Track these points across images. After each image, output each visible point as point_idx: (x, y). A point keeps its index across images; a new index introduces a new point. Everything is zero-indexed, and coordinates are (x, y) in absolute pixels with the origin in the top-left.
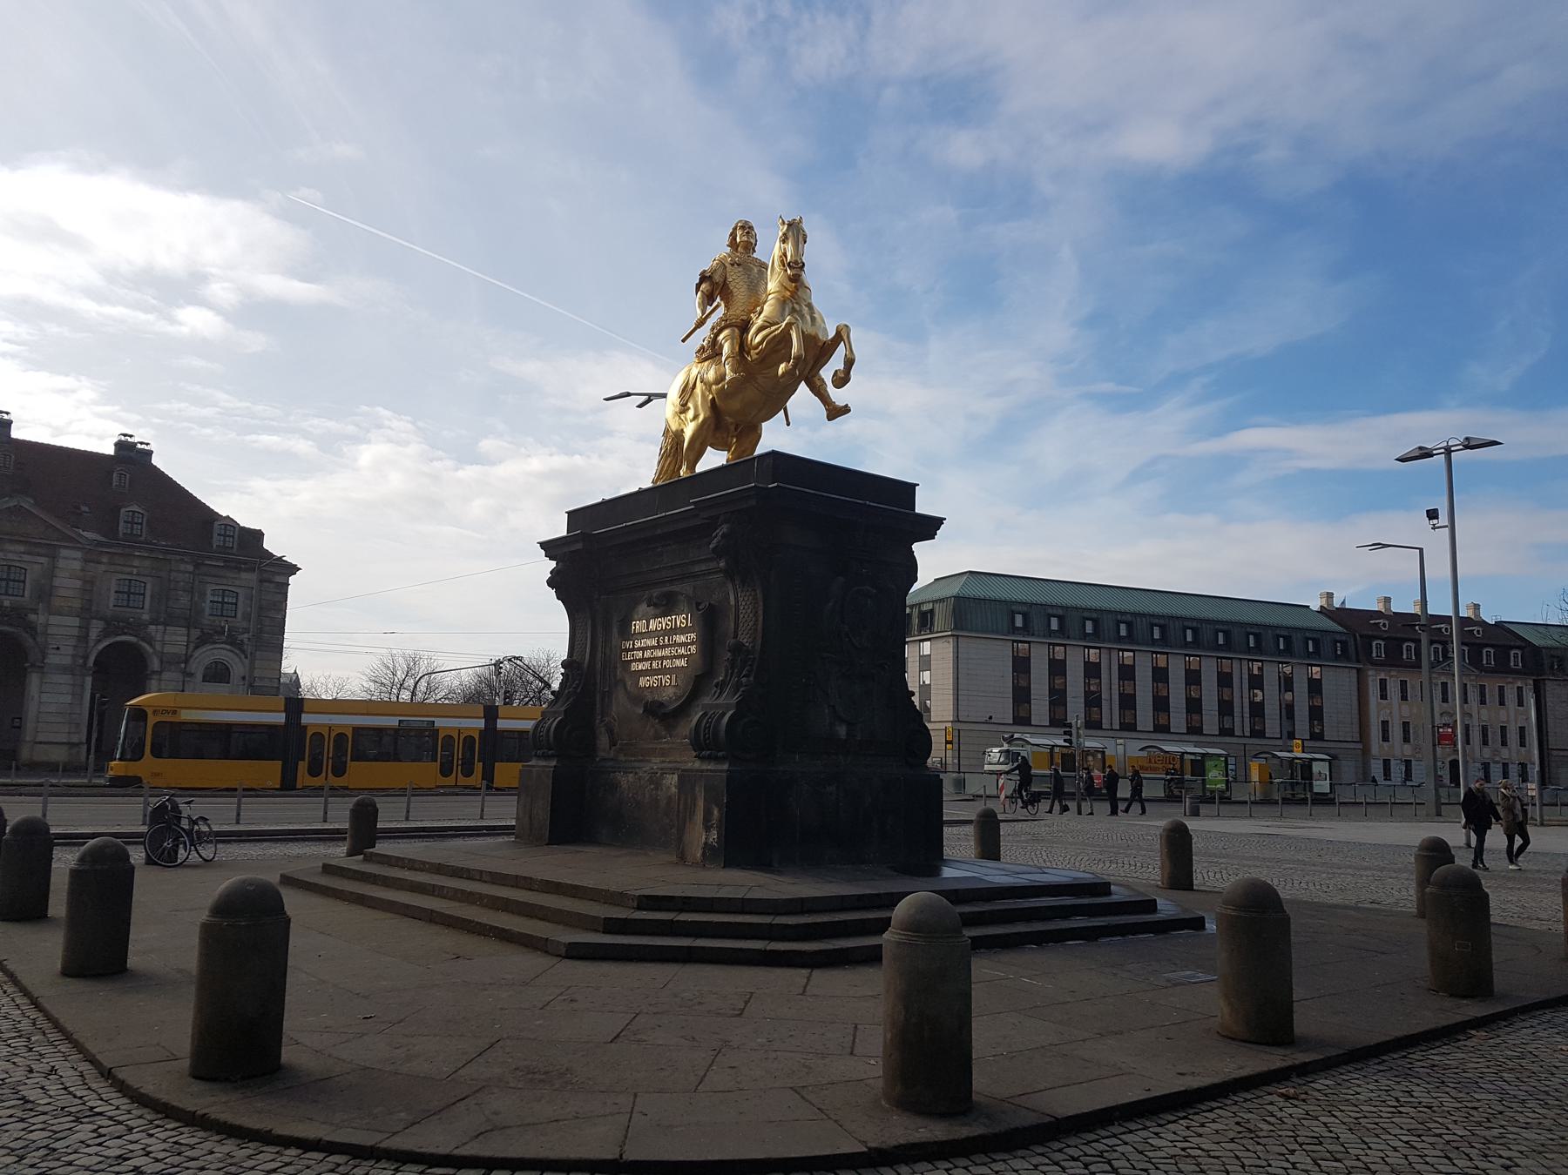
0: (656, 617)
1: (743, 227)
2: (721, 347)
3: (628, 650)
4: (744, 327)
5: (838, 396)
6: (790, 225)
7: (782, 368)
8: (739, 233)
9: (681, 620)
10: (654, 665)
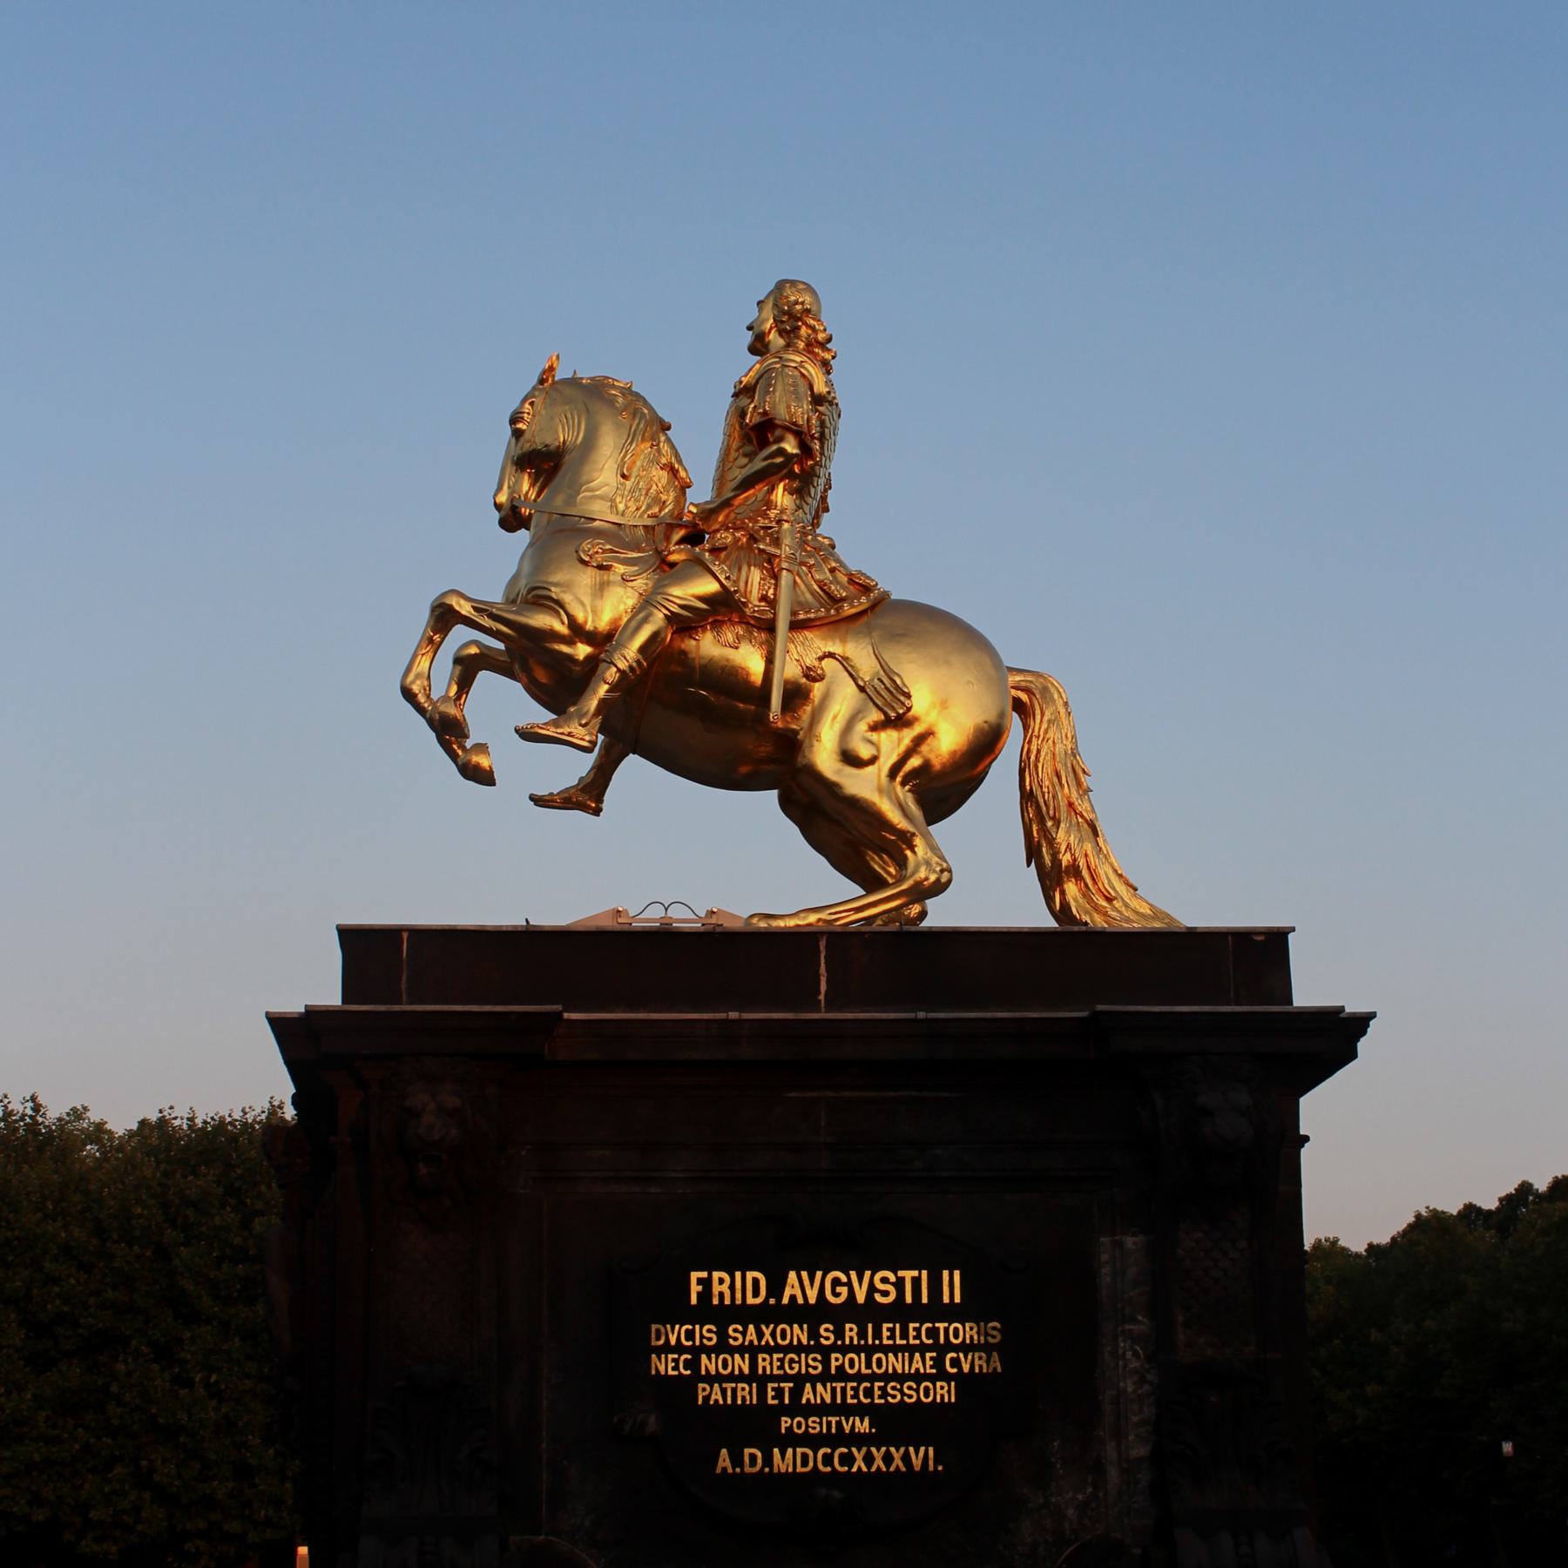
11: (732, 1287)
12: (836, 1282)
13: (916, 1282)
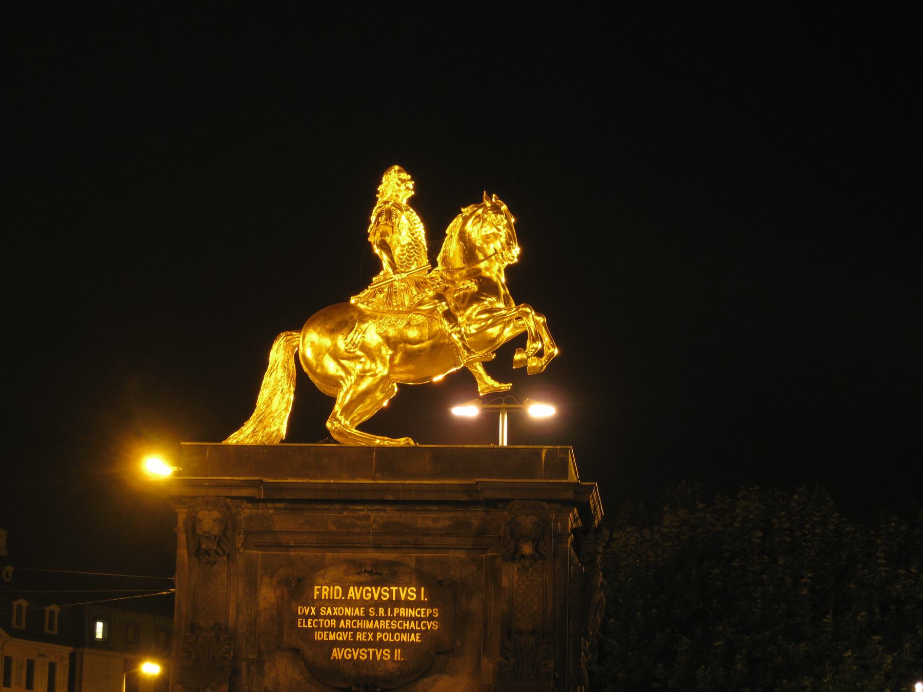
0: (359, 584)
3: (307, 617)
9: (409, 593)
10: (360, 636)
11: (329, 593)
12: (367, 591)
13: (397, 591)
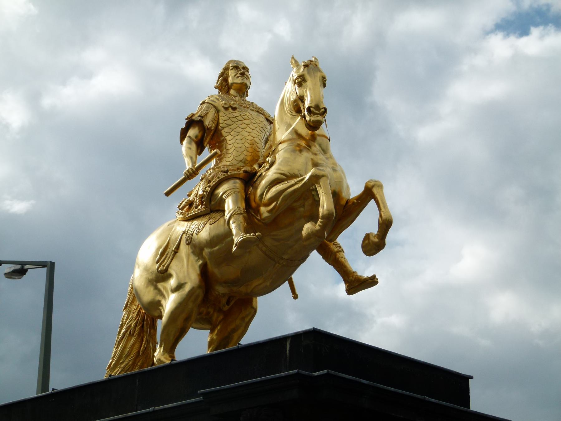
1: (236, 67)
2: (222, 202)
4: (249, 179)
5: (362, 266)
6: (306, 66)
7: (308, 227)
8: (232, 73)
